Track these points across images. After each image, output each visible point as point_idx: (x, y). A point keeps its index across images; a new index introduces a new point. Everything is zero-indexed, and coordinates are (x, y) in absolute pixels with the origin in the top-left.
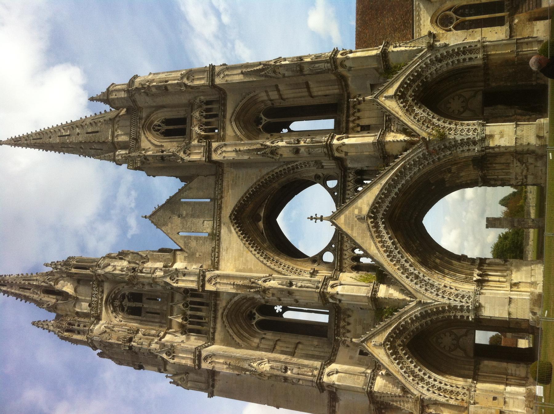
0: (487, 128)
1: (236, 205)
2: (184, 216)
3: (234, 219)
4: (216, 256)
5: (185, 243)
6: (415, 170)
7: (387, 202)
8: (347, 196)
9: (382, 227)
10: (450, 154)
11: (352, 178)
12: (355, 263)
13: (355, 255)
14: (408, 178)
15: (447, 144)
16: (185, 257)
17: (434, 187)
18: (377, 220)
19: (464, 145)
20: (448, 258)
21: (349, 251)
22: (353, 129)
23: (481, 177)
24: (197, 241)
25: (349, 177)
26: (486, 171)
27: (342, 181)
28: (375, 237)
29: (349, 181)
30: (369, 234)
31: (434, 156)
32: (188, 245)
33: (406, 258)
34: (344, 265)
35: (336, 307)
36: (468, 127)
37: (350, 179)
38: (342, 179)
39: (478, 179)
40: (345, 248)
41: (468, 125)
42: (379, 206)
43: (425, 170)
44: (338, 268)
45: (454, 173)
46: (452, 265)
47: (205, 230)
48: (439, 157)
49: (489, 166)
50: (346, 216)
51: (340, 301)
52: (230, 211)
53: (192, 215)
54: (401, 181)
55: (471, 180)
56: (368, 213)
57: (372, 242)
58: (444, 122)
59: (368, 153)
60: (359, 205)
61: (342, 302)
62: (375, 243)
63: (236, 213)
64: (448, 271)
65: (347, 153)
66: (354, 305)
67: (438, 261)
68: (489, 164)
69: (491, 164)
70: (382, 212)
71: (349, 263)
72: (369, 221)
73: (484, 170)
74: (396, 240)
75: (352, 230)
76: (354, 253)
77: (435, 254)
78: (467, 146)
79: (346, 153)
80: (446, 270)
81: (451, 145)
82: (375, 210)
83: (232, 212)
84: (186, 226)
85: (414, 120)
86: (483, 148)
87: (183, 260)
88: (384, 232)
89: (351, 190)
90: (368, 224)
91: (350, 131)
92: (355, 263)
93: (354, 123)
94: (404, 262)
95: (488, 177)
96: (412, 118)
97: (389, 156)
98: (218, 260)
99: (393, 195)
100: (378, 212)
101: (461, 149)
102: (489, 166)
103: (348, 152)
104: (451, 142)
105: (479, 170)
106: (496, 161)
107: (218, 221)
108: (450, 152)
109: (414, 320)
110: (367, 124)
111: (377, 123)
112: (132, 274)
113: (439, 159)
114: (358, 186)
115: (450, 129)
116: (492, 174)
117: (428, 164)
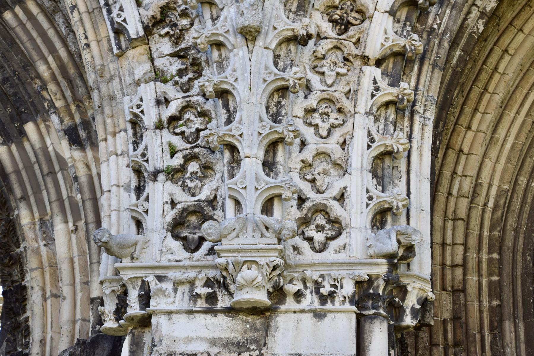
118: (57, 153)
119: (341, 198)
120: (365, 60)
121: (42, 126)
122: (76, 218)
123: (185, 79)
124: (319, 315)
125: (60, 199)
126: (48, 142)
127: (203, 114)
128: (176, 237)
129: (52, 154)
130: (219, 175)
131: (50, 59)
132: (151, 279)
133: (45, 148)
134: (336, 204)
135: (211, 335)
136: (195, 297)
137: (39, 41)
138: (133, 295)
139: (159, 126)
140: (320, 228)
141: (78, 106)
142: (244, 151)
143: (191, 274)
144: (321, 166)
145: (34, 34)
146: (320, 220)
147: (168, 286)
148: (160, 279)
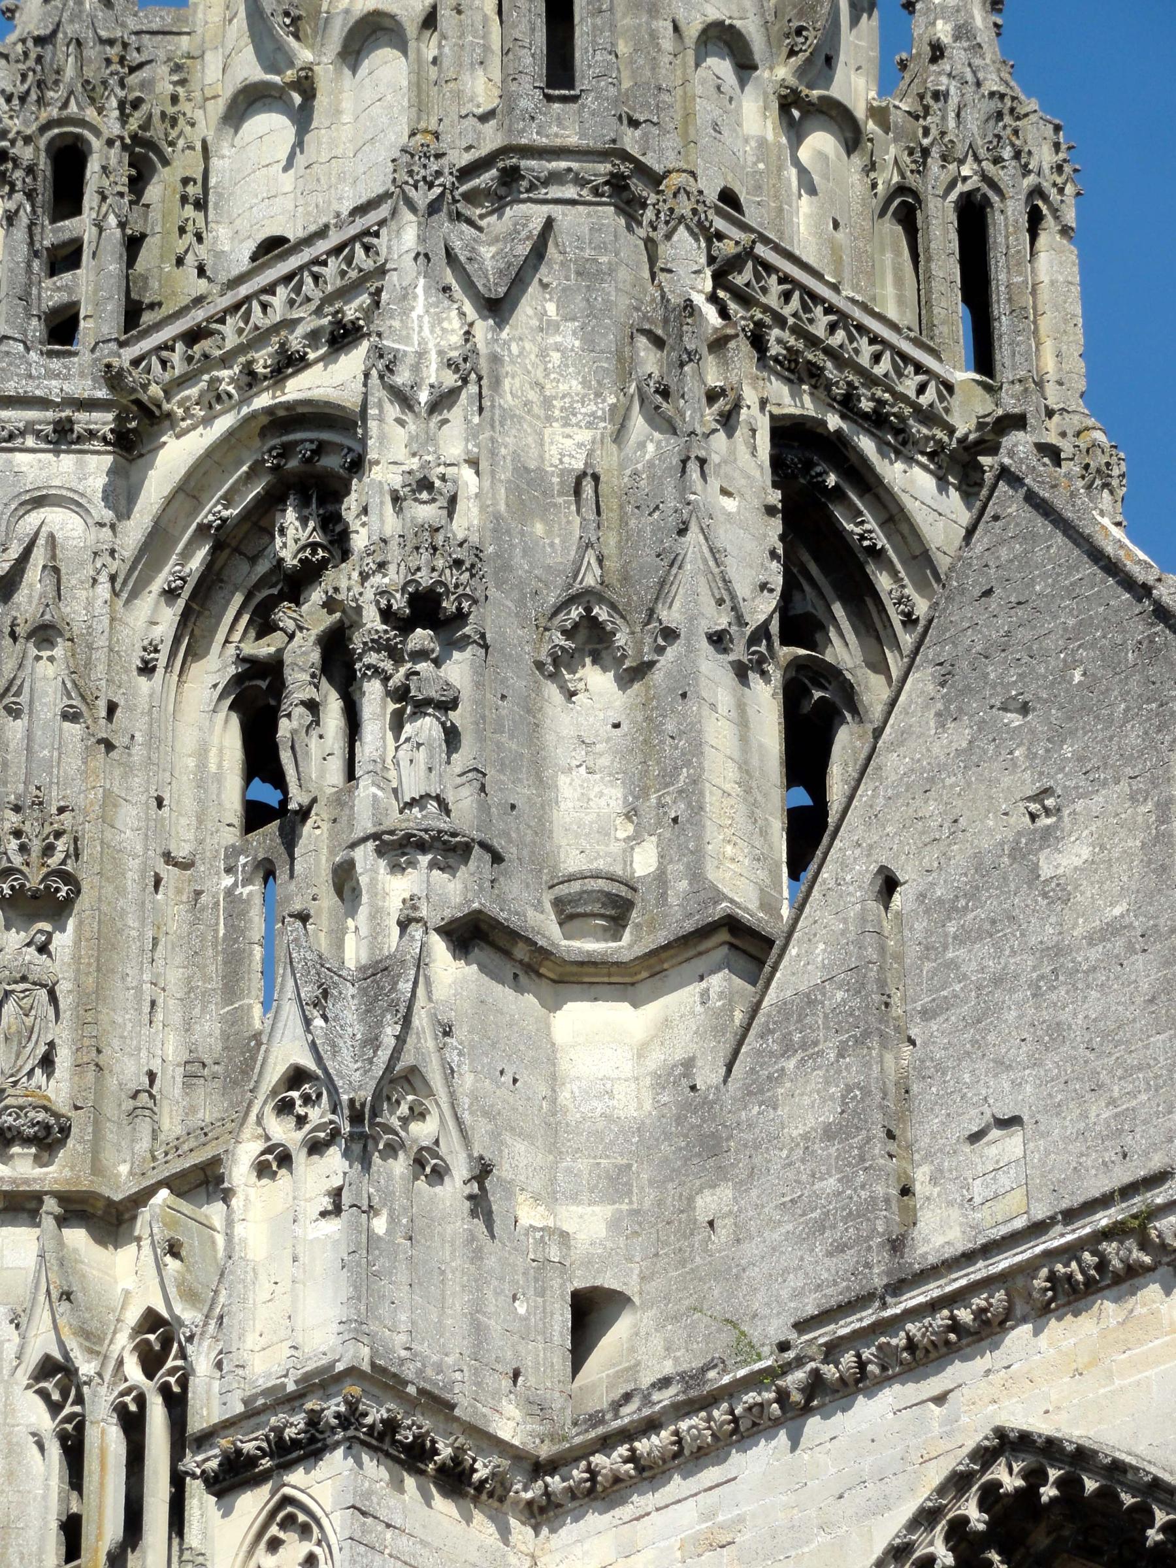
1: (1117, 1470)
2: (1046, 871)
3: (990, 1496)
4: (642, 1446)
5: (809, 1000)
16: (689, 1064)
24: (829, 1133)
32: (788, 1049)
47: (934, 1180)
52: (1041, 1426)
53: (1058, 951)
63: (1048, 1492)
83: (1051, 1449)
84: (963, 938)
87: (656, 1059)
98: (617, 1479)
107: (941, 1319)
112: (372, 620)
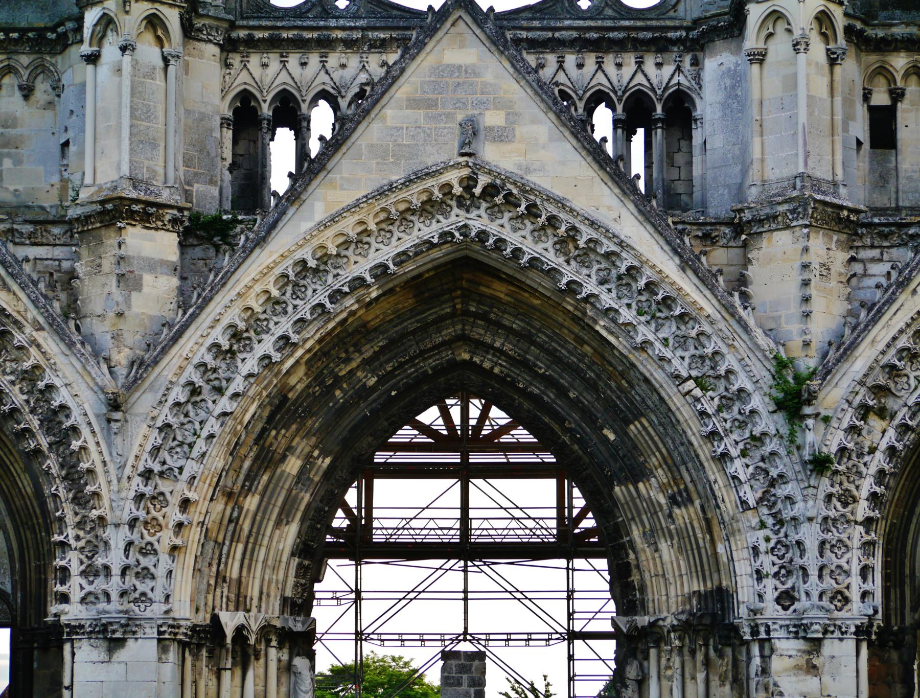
0: (850, 644)
6: (676, 362)
7: (539, 248)
8: (571, 60)
9: (429, 230)
10: (744, 503)
11: (655, 81)
12: (266, 110)
13: (304, 107)
14: (644, 332)
15: (781, 491)
17: (612, 437)
18: (456, 210)
19: (781, 557)
20: (308, 505)
21: (323, 77)
22: (883, 71)
23: (653, 624)
25: (659, 65)
26: (677, 643)
27: (641, 35)
28: (383, 203)
29: (640, 64)
30: (397, 176)
31: (735, 436)
33: (295, 338)
34: (255, 60)
35: (65, 35)
36: (855, 568)
37: (649, 66)
38: (649, 35)
39: (646, 612)
40: (333, 60)
41: (865, 572)
42: (521, 217)
43: (676, 401)
44: (242, 33)
45: (670, 516)
46: (278, 524)
48: (732, 459)
49: (700, 657)
50: (471, 71)
51: (93, 59)
54: (629, 306)
55: (643, 589)
56: (490, 172)
57: (360, 196)
58: (881, 473)
59: (756, 154)
60: (522, 130)
61: (90, 68)
62: (356, 205)
64: (253, 508)
65: (761, 62)
66: (75, 113)
67: (293, 465)
68: (707, 655)
69: (707, 663)
70: (493, 228)
71: (267, 81)
72: (453, 177)
73: (681, 638)
74: (374, 295)
75: (414, 103)
76: (314, 102)
77: (324, 454)
78: (776, 569)
79: (758, 58)
80: (257, 498)
81: (779, 505)
82: (499, 199)
85: (893, 351)
86: (768, 632)
88: (407, 241)
89: (600, 75)
90: (439, 172)
91: (873, 59)
92: (266, 110)
93: (906, 75)
94: (279, 332)
95: (653, 652)
96: (903, 342)
97: (745, 245)
99: (569, 273)
100: (494, 212)
101: (763, 547)
102: (700, 657)
103: (766, 64)
104: (793, 503)
105: (683, 617)
106: (715, 682)
108: (752, 503)
109: (33, 381)
110: (902, 134)
111: (902, 181)
113: (724, 458)
114: (620, 108)
115: (848, 499)
116: (668, 667)
117: (703, 414)
118: (657, 501)
119: (848, 587)
120: (856, 522)
121: (647, 484)
122: (672, 538)
123: (777, 528)
124: (841, 640)
125: (662, 528)
126: (652, 494)
127: (786, 546)
128: (778, 604)
129: (654, 501)
130: (795, 577)
131: (657, 454)
132: (770, 623)
133: (650, 497)
134: (845, 590)
135: (797, 648)
136: (790, 632)
137: (650, 442)
138: (762, 629)
139: (767, 553)
140: (839, 601)
141: (675, 483)
142: (810, 572)
143: (788, 622)
144: (838, 572)
145: (647, 438)
146: (839, 597)
147: (776, 627)
148: (774, 623)
